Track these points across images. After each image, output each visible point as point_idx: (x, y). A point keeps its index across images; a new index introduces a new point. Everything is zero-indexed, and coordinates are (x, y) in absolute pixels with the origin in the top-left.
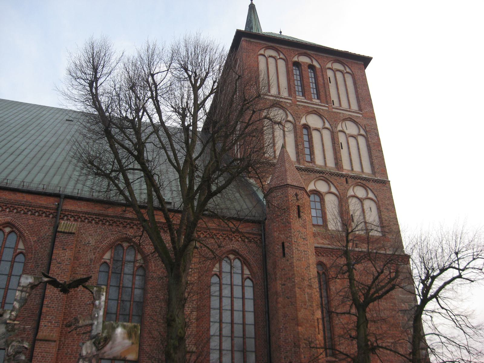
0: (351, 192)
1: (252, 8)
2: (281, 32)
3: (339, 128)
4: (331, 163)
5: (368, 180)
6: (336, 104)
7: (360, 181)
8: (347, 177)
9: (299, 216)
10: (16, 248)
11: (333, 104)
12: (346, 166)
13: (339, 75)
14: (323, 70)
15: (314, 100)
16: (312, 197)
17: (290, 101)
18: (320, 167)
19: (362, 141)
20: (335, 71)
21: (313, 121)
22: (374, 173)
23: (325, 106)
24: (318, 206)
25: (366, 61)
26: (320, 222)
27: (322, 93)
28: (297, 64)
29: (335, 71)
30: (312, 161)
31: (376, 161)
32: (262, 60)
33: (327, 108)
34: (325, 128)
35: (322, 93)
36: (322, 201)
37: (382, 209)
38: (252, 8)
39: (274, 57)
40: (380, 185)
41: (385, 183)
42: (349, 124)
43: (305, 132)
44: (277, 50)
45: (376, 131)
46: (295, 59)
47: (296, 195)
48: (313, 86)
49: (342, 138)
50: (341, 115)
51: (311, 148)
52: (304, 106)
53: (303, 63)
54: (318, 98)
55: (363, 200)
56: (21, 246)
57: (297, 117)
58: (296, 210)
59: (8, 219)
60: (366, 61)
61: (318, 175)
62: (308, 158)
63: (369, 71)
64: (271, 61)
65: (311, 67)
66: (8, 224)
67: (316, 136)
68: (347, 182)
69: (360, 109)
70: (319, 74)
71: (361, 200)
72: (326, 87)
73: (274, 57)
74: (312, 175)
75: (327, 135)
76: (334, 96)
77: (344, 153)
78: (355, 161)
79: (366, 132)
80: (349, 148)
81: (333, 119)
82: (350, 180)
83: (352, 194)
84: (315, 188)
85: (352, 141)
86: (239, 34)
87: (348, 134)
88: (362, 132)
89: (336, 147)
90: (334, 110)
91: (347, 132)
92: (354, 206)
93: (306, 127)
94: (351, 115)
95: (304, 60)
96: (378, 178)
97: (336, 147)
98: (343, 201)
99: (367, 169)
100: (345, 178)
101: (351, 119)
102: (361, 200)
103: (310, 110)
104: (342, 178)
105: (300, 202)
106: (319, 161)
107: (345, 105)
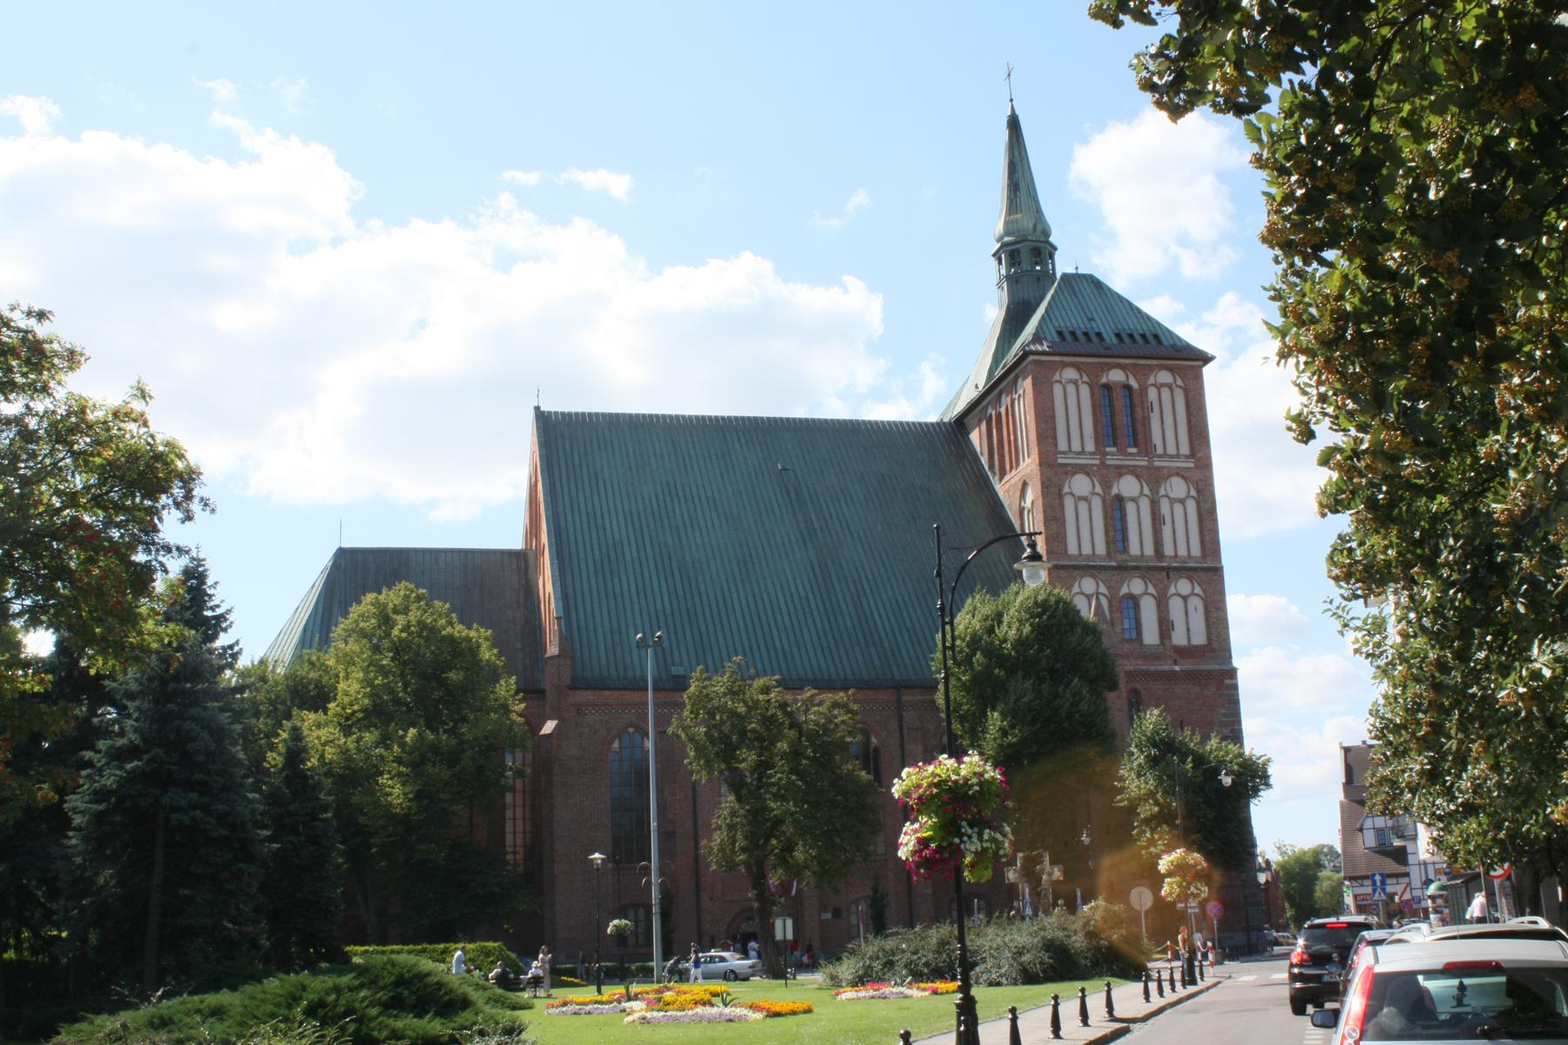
0: (1172, 590)
1: (1014, 124)
3: (1162, 492)
4: (1149, 550)
6: (1160, 451)
8: (1168, 570)
12: (1168, 550)
13: (1165, 392)
14: (1144, 390)
18: (1136, 558)
20: (1159, 387)
21: (1128, 486)
22: (1204, 556)
24: (1132, 612)
25: (1206, 359)
26: (1134, 636)
30: (1125, 550)
35: (1140, 437)
36: (1137, 607)
38: (1014, 124)
46: (1104, 380)
54: (1135, 445)
57: (1107, 486)
60: (1206, 359)
62: (1120, 545)
64: (1071, 388)
65: (1128, 387)
67: (1130, 508)
69: (1192, 455)
70: (1137, 400)
71: (1185, 598)
72: (1146, 421)
73: (1075, 383)
75: (1145, 505)
78: (1182, 542)
79: (1198, 491)
81: (1154, 478)
82: (1172, 574)
85: (1178, 508)
88: (1193, 493)
89: (1157, 520)
91: (1172, 495)
92: (1175, 606)
93: (1120, 499)
96: (1209, 564)
99: (1196, 551)
101: (1178, 474)
102: (1185, 598)
106: (1134, 549)
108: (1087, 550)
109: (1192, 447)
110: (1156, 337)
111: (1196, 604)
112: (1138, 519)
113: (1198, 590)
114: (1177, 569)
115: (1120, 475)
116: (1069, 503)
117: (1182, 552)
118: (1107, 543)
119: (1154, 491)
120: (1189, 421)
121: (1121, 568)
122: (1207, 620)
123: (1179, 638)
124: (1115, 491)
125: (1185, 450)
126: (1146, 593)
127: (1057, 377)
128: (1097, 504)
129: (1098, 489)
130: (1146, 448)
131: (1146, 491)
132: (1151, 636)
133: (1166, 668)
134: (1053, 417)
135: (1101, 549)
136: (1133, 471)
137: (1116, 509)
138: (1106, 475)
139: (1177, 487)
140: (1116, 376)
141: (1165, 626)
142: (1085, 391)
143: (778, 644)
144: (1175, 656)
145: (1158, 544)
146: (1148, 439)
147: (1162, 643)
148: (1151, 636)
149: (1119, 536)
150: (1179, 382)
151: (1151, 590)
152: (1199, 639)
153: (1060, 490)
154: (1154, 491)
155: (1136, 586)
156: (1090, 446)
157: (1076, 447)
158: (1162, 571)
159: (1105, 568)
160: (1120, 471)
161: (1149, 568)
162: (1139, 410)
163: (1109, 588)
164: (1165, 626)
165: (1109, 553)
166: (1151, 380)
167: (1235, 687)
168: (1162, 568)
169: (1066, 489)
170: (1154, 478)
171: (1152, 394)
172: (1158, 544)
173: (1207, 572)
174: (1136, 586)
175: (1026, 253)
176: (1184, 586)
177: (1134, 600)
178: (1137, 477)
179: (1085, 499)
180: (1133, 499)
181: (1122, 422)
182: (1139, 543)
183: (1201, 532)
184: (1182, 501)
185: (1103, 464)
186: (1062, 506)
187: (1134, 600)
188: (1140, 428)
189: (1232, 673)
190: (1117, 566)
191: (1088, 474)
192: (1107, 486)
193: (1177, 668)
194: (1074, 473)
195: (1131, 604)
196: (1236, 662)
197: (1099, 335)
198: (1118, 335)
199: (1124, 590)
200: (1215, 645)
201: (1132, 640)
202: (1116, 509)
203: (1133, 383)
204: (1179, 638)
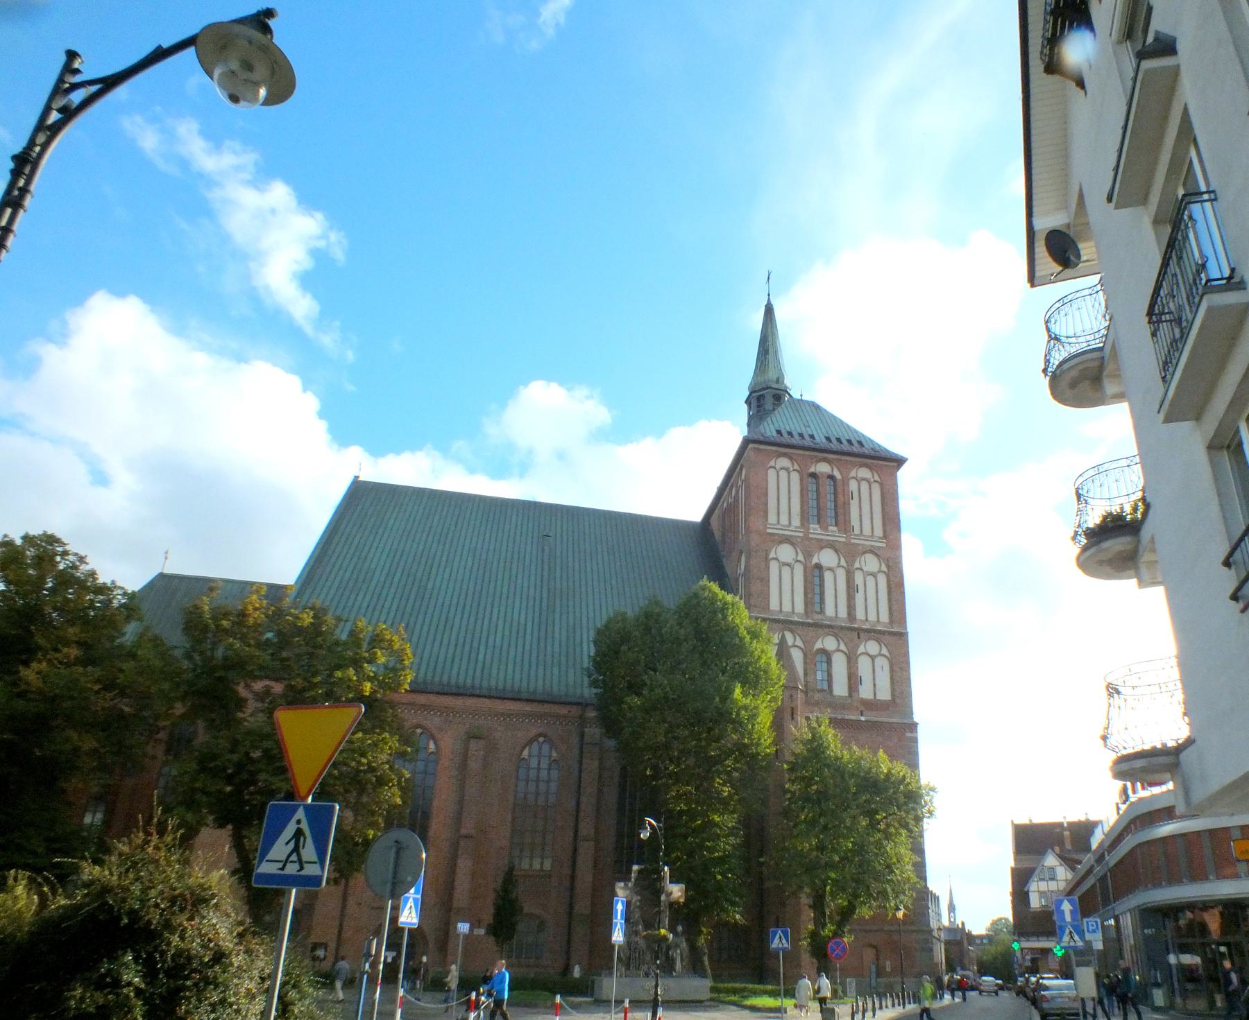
0: (861, 649)
3: (857, 565)
4: (843, 613)
5: (883, 633)
6: (857, 531)
7: (873, 633)
10: (550, 756)
12: (860, 615)
13: (864, 486)
14: (845, 482)
15: (831, 528)
16: (818, 658)
18: (830, 619)
19: (882, 580)
20: (859, 480)
21: (827, 558)
22: (891, 622)
24: (825, 666)
25: (899, 461)
26: (826, 687)
27: (841, 518)
28: (813, 475)
29: (859, 480)
30: (822, 611)
31: (895, 607)
32: (772, 473)
34: (839, 566)
35: (841, 518)
36: (829, 662)
37: (895, 668)
39: (787, 469)
41: (902, 636)
42: (869, 557)
43: (816, 572)
44: (791, 459)
46: (812, 470)
48: (831, 505)
49: (859, 579)
51: (822, 594)
52: (818, 540)
53: (822, 473)
54: (836, 525)
56: (554, 754)
57: (808, 555)
59: (541, 730)
60: (899, 461)
63: (903, 474)
64: (783, 474)
65: (831, 477)
66: (540, 735)
67: (828, 576)
69: (885, 537)
70: (840, 490)
71: (873, 658)
72: (846, 505)
73: (787, 469)
74: (820, 631)
75: (841, 574)
76: (854, 521)
77: (859, 598)
78: (873, 609)
79: (888, 567)
81: (850, 553)
82: (862, 635)
85: (871, 581)
86: (746, 442)
88: (884, 568)
89: (851, 589)
92: (864, 666)
93: (818, 566)
95: (823, 468)
97: (851, 589)
98: (852, 660)
99: (885, 617)
101: (871, 552)
102: (873, 658)
106: (829, 611)
108: (787, 607)
109: (884, 531)
110: (860, 443)
111: (882, 663)
112: (835, 586)
113: (884, 651)
115: (822, 548)
116: (774, 567)
117: (872, 617)
118: (806, 604)
120: (883, 510)
121: (816, 625)
122: (892, 678)
123: (865, 692)
124: (815, 560)
125: (879, 532)
126: (838, 650)
127: (772, 463)
128: (799, 570)
129: (801, 558)
131: (843, 563)
132: (840, 688)
133: (853, 718)
134: (766, 495)
135: (800, 607)
136: (832, 546)
137: (814, 576)
138: (807, 546)
140: (823, 468)
141: (854, 681)
142: (795, 477)
143: (481, 657)
145: (851, 607)
146: (847, 521)
147: (850, 695)
148: (840, 688)
149: (817, 598)
150: (877, 478)
151: (843, 647)
152: (884, 694)
153: (767, 555)
154: (851, 562)
155: (829, 643)
156: (796, 522)
157: (784, 520)
158: (853, 632)
159: (802, 624)
160: (822, 545)
162: (840, 496)
164: (854, 681)
165: (806, 612)
166: (853, 474)
167: (915, 740)
169: (772, 555)
171: (853, 485)
172: (851, 607)
173: (894, 638)
174: (829, 643)
175: (766, 396)
176: (872, 647)
178: (836, 551)
179: (788, 565)
180: (830, 569)
181: (826, 504)
182: (835, 606)
183: (890, 600)
184: (874, 575)
185: (806, 537)
186: (768, 568)
188: (840, 511)
189: (913, 727)
190: (813, 624)
191: (792, 544)
192: (808, 555)
193: (863, 719)
194: (781, 543)
195: (824, 659)
196: (916, 718)
197: (812, 437)
198: (828, 439)
199: (818, 645)
200: (898, 701)
201: (823, 691)
202: (814, 576)
203: (838, 476)
204: (865, 692)
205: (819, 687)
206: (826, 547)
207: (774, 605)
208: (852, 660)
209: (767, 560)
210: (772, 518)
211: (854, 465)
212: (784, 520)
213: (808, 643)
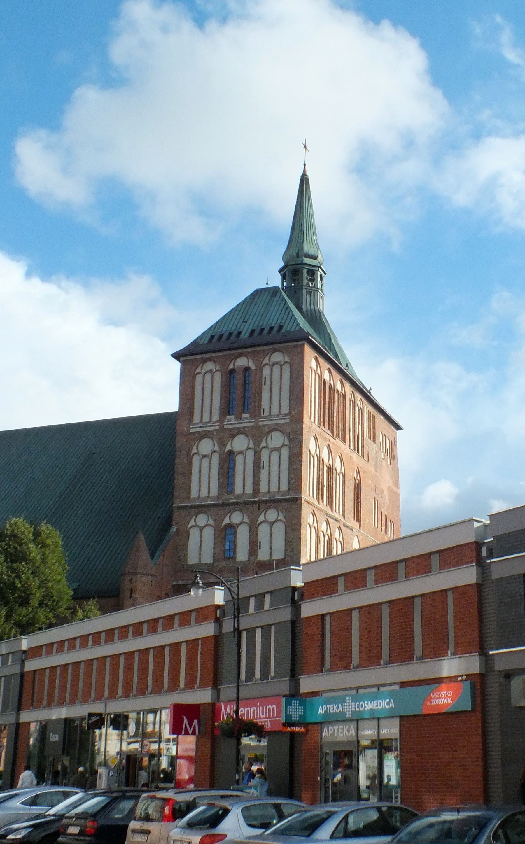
0: (261, 518)
1: (304, 181)
2: (267, 284)
4: (249, 490)
6: (266, 413)
8: (260, 502)
9: (131, 596)
11: (264, 414)
12: (263, 488)
14: (260, 369)
17: (217, 428)
18: (238, 497)
19: (285, 452)
23: (251, 422)
30: (232, 492)
33: (252, 424)
38: (304, 181)
39: (210, 371)
40: (290, 503)
45: (300, 437)
46: (231, 366)
47: (131, 580)
49: (264, 456)
50: (266, 428)
52: (231, 430)
53: (238, 368)
55: (273, 524)
57: (222, 445)
58: (129, 592)
61: (232, 507)
67: (239, 460)
68: (259, 509)
71: (272, 524)
74: (227, 509)
75: (250, 455)
76: (265, 405)
77: (264, 473)
79: (290, 440)
80: (270, 466)
82: (262, 506)
83: (264, 519)
84: (229, 522)
87: (272, 448)
88: (287, 442)
89: (257, 466)
90: (260, 423)
93: (231, 453)
94: (276, 424)
97: (257, 466)
98: (254, 530)
99: (284, 487)
100: (257, 506)
103: (235, 433)
104: (254, 505)
105: (133, 585)
106: (238, 490)
107: (275, 411)
108: (204, 493)
111: (279, 527)
112: (243, 467)
114: (266, 502)
115: (233, 436)
116: (196, 460)
119: (257, 444)
121: (225, 505)
124: (228, 448)
125: (285, 410)
130: (256, 412)
135: (214, 492)
138: (223, 436)
139: (277, 439)
141: (254, 546)
144: (257, 569)
145: (256, 483)
154: (257, 444)
156: (216, 417)
157: (206, 418)
158: (256, 505)
160: (234, 434)
161: (246, 503)
163: (215, 520)
164: (254, 546)
168: (255, 502)
169: (194, 450)
170: (258, 435)
171: (266, 371)
172: (256, 483)
177: (232, 528)
180: (240, 453)
182: (242, 485)
186: (190, 463)
187: (232, 528)
192: (222, 445)
194: (201, 438)
199: (226, 521)
203: (252, 366)
204: (263, 555)
205: (227, 555)
206: (237, 434)
207: (194, 493)
208: (254, 530)
209: (189, 457)
210: (196, 419)
211: (265, 353)
212: (206, 418)
213: (218, 521)
